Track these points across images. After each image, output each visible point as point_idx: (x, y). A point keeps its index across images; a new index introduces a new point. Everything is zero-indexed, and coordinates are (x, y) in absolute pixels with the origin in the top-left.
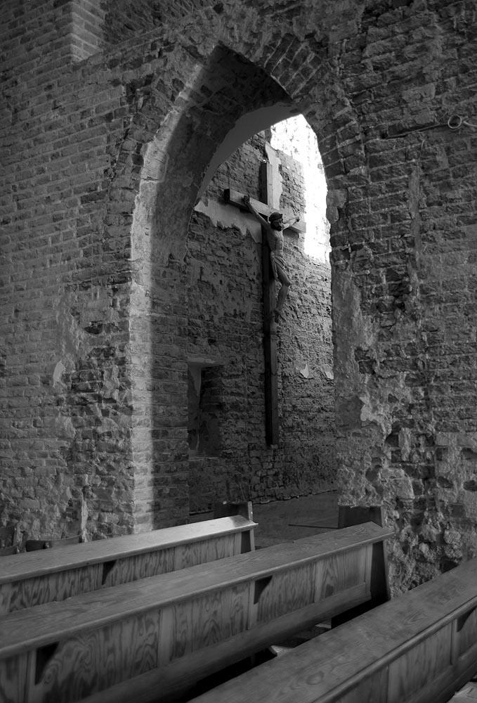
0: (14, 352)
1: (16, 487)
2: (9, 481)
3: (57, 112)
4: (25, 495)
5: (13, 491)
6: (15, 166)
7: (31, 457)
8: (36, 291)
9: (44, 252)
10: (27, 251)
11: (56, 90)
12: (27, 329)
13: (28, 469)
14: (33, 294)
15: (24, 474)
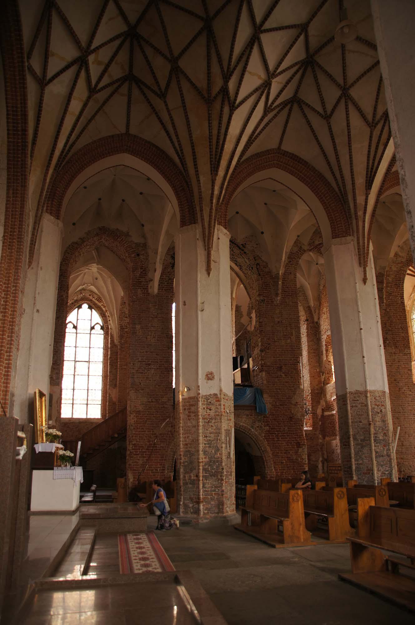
0: (406, 441)
1: (409, 470)
2: (407, 469)
3: (411, 392)
4: (412, 471)
5: (408, 471)
6: (401, 400)
7: (413, 463)
8: (411, 429)
9: (411, 421)
10: (406, 420)
11: (410, 387)
12: (409, 436)
13: (412, 466)
14: (410, 429)
15: (411, 467)
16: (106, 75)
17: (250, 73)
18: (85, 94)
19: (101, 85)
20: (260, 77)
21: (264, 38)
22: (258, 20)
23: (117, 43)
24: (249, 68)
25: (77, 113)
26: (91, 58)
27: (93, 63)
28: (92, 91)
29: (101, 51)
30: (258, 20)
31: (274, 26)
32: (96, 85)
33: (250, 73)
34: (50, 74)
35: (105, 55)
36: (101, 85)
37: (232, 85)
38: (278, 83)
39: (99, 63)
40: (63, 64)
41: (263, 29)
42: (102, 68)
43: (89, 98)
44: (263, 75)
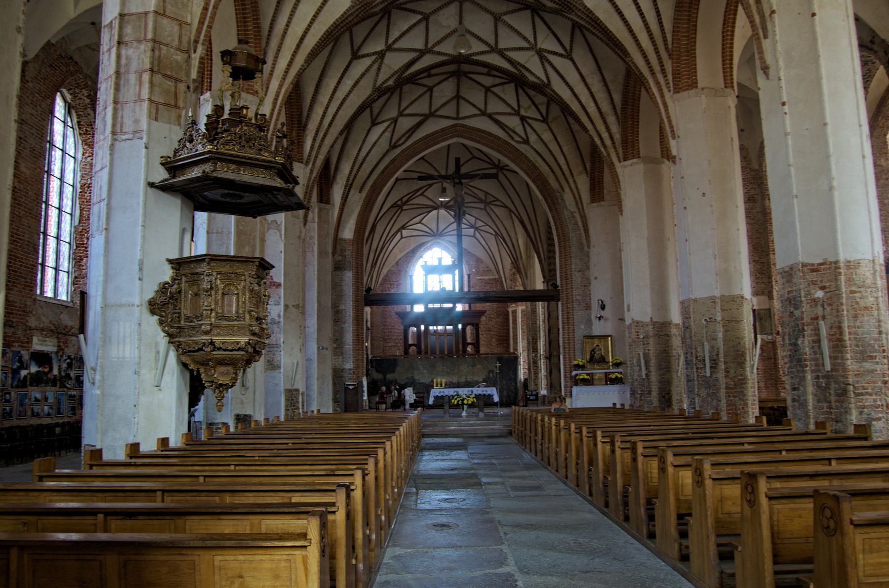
16: (539, 106)
17: (527, 62)
18: (544, 126)
19: (544, 113)
20: (533, 56)
21: (501, 45)
22: (486, 48)
23: (520, 91)
24: (522, 62)
25: (552, 137)
26: (523, 113)
27: (526, 112)
28: (545, 120)
29: (521, 103)
30: (486, 48)
31: (493, 37)
32: (542, 116)
33: (527, 62)
34: (524, 136)
35: (525, 102)
36: (544, 113)
37: (531, 78)
38: (546, 38)
39: (529, 107)
40: (521, 126)
41: (494, 46)
42: (533, 107)
43: (548, 125)
44: (532, 53)
